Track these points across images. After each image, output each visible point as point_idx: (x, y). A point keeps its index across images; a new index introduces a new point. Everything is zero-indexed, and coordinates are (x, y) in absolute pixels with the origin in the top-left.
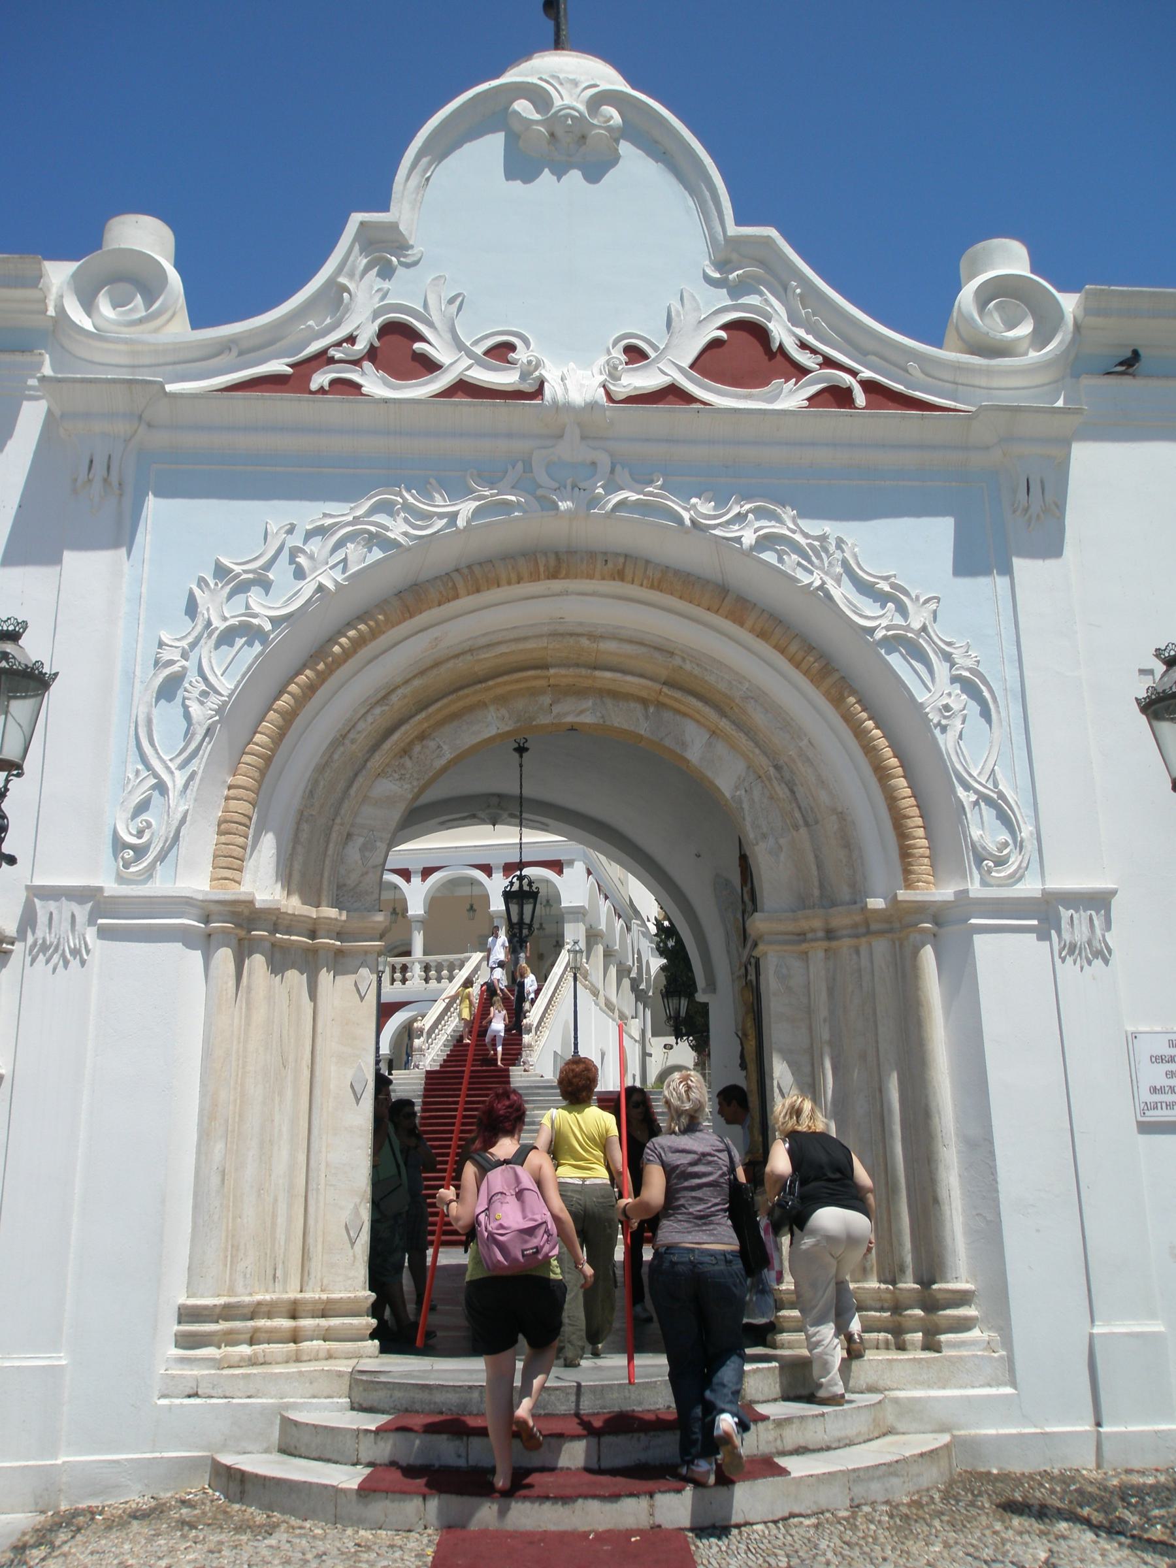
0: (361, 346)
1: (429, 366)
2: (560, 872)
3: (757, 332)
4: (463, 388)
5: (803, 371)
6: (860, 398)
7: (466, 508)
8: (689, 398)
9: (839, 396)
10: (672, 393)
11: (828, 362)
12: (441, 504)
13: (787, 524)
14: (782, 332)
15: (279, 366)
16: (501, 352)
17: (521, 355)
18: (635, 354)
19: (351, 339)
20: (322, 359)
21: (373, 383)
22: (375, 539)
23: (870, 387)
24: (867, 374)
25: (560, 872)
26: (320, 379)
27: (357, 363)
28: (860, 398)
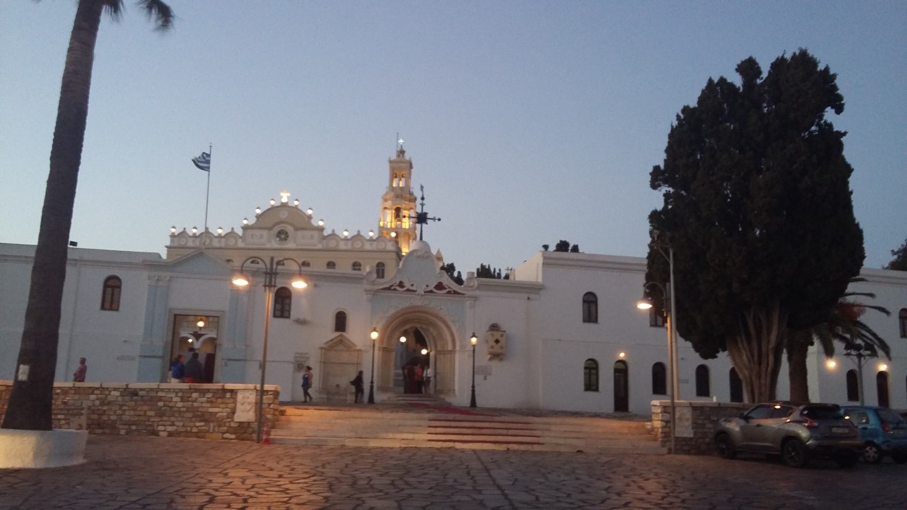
0: (396, 284)
4: (408, 290)
6: (452, 292)
8: (434, 293)
9: (449, 292)
10: (431, 292)
11: (449, 288)
14: (444, 284)
15: (387, 286)
16: (412, 285)
18: (427, 286)
19: (395, 283)
20: (392, 286)
21: (398, 288)
26: (393, 288)
27: (396, 286)
28: (452, 292)
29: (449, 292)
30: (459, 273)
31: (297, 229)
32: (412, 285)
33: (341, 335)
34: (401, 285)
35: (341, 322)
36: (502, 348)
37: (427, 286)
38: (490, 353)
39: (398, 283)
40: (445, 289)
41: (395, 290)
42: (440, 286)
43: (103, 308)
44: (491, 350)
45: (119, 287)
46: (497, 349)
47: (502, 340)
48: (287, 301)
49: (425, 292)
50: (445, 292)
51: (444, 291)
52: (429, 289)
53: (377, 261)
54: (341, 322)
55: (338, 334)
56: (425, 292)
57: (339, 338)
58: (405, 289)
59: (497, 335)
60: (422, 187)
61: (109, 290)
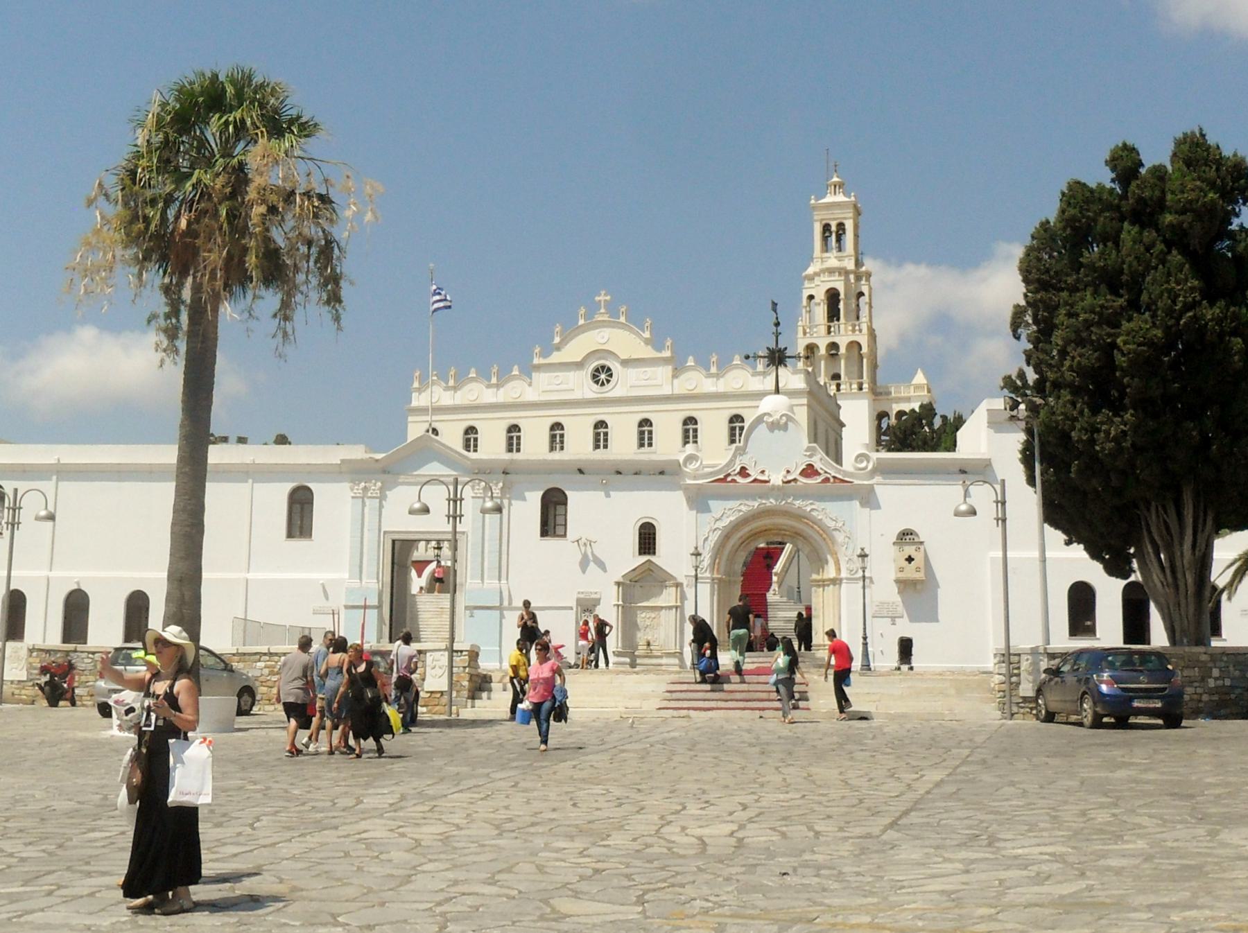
1: (748, 475)
3: (810, 466)
4: (755, 480)
5: (820, 474)
6: (832, 480)
7: (756, 504)
10: (795, 480)
11: (826, 472)
12: (750, 503)
13: (817, 505)
15: (722, 476)
16: (763, 472)
17: (766, 473)
18: (788, 472)
21: (739, 479)
22: (740, 511)
23: (834, 477)
24: (833, 474)
26: (729, 479)
28: (832, 480)
29: (826, 480)
31: (626, 363)
32: (763, 472)
33: (649, 561)
34: (743, 472)
35: (647, 539)
36: (918, 570)
37: (788, 472)
38: (898, 581)
39: (738, 470)
40: (820, 474)
41: (733, 481)
42: (810, 471)
43: (290, 535)
44: (901, 575)
45: (311, 502)
46: (911, 572)
47: (919, 557)
48: (560, 509)
49: (784, 482)
50: (819, 480)
51: (819, 479)
52: (790, 478)
54: (647, 539)
55: (645, 558)
56: (784, 482)
57: (647, 566)
58: (750, 479)
59: (910, 550)
60: (775, 305)
61: (297, 507)
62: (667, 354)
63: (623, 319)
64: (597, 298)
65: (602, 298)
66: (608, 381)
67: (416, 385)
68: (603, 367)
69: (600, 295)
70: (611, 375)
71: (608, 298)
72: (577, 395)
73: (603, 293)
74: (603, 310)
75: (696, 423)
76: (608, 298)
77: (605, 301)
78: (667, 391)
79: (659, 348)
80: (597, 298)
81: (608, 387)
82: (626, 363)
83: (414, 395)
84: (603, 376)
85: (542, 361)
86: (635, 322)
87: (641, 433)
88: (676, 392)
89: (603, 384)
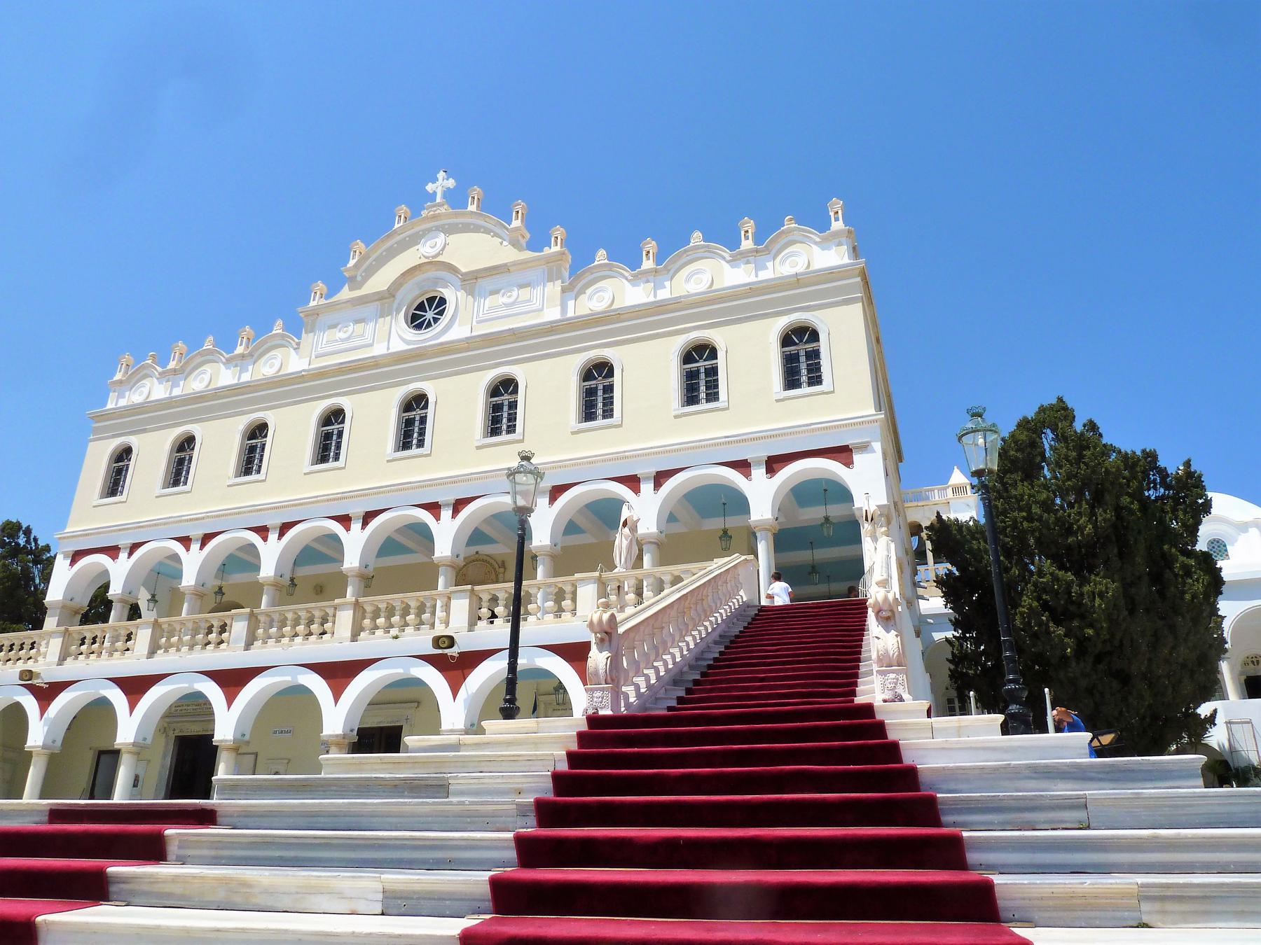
2: (848, 463)
25: (848, 463)
30: (1092, 426)
31: (472, 281)
53: (781, 323)
62: (556, 249)
63: (472, 208)
64: (430, 187)
65: (441, 184)
66: (436, 320)
67: (118, 376)
68: (431, 300)
69: (435, 180)
70: (441, 313)
71: (451, 183)
72: (379, 350)
73: (441, 175)
74: (438, 200)
75: (611, 373)
76: (451, 183)
77: (448, 193)
78: (552, 314)
79: (537, 243)
80: (430, 187)
81: (436, 328)
82: (472, 281)
83: (113, 395)
84: (430, 315)
85: (323, 301)
86: (497, 208)
87: (497, 408)
88: (570, 314)
89: (429, 325)
